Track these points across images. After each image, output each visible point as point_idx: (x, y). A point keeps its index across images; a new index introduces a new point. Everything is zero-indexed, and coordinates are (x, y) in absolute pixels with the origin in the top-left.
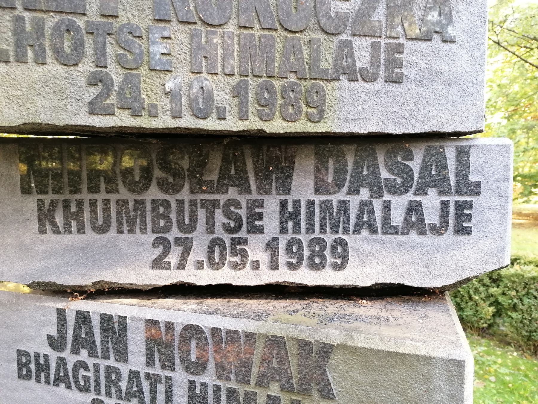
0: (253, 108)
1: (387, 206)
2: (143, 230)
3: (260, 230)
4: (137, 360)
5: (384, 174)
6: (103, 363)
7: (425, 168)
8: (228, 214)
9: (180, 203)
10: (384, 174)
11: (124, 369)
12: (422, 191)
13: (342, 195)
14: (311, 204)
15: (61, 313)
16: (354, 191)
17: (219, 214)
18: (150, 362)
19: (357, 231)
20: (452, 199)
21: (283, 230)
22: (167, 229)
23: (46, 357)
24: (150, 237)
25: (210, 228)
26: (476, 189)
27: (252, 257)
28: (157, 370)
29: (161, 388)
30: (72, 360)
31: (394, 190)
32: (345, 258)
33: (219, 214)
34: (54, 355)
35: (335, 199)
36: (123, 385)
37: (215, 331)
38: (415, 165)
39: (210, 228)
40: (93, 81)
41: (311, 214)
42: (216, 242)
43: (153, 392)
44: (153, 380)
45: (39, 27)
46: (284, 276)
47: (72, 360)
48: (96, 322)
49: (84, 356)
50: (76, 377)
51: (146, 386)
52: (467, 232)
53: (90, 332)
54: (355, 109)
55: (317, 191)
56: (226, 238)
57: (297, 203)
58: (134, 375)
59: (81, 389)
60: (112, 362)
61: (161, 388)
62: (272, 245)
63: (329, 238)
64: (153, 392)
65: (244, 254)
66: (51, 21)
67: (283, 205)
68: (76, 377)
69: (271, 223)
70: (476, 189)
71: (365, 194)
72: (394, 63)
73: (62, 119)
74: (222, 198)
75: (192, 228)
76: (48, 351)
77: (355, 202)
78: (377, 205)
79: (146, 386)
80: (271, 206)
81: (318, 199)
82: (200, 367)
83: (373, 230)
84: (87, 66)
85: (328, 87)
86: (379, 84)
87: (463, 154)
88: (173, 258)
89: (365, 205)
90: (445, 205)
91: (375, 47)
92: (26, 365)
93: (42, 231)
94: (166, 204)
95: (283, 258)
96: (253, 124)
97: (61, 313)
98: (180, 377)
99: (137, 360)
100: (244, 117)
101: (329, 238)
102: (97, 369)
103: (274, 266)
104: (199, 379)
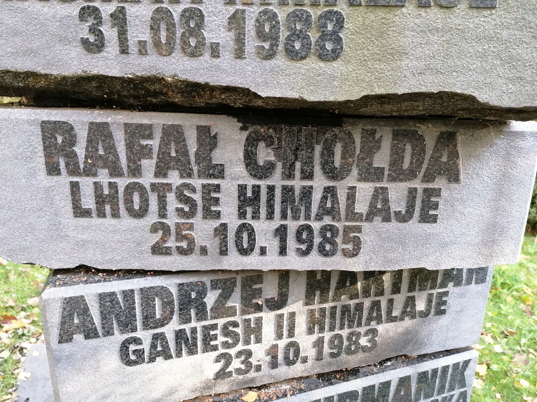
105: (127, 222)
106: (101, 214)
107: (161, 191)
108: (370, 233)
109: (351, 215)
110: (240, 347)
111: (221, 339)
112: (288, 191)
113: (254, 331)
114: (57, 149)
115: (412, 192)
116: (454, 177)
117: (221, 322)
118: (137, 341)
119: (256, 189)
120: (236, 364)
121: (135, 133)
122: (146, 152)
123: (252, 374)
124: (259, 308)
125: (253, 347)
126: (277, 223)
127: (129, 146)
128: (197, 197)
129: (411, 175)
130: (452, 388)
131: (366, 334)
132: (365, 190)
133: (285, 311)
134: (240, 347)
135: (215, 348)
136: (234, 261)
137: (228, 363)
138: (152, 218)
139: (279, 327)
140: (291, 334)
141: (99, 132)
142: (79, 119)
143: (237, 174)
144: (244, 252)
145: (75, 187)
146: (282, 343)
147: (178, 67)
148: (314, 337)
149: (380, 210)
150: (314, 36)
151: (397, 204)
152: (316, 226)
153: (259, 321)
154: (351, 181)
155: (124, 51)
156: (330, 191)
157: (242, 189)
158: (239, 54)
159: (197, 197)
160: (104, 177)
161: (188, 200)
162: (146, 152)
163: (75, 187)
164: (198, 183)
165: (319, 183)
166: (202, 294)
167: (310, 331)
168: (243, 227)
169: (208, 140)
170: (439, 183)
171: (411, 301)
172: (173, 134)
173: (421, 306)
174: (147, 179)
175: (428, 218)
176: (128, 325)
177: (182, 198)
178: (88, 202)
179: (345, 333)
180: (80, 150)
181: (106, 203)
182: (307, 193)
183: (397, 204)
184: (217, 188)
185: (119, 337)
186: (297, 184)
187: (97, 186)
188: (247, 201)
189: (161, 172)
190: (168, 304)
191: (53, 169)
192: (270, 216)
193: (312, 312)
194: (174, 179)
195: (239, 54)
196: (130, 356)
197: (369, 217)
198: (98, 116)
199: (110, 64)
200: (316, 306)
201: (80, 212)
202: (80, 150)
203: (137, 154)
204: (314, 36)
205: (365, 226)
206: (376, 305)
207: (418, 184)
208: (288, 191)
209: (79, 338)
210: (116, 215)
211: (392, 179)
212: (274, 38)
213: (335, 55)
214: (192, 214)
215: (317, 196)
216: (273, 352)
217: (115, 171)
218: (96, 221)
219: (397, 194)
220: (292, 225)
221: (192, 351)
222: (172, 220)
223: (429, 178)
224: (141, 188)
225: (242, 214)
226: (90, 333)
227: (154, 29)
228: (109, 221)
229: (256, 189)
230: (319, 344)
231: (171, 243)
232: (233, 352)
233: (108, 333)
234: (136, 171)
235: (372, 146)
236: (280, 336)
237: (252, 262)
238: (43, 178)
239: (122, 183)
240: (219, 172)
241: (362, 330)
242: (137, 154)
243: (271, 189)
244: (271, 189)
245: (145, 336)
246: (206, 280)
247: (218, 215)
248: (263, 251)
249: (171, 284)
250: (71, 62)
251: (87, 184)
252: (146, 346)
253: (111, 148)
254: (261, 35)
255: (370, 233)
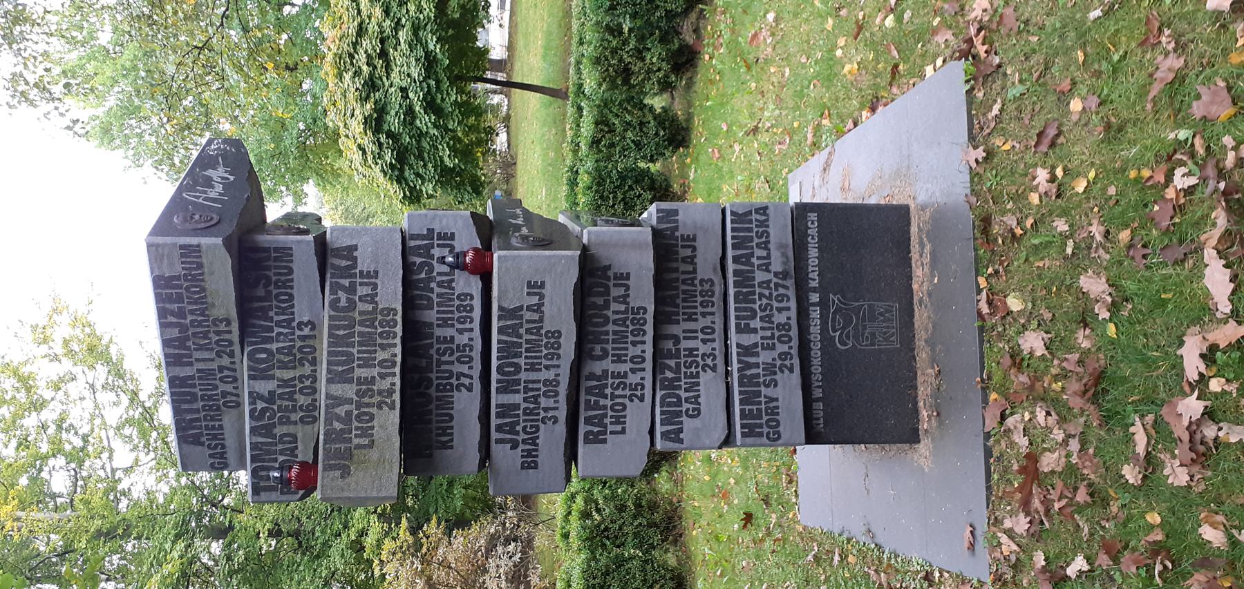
0: (391, 341)
1: (439, 274)
2: (452, 397)
3: (452, 338)
4: (518, 398)
5: (423, 275)
6: (522, 418)
7: (420, 255)
8: (444, 354)
9: (437, 378)
10: (423, 275)
11: (524, 405)
12: (432, 257)
13: (434, 297)
14: (438, 312)
15: (498, 441)
16: (432, 290)
17: (443, 359)
18: (518, 392)
19: (453, 289)
20: (436, 242)
21: (453, 326)
22: (451, 385)
23: (523, 451)
24: (456, 393)
25: (452, 363)
26: (431, 231)
27: (466, 341)
28: (521, 387)
29: (530, 386)
30: (522, 436)
31: (431, 270)
32: (468, 294)
33: (443, 359)
34: (521, 447)
35: (436, 300)
36: (532, 406)
37: (498, 359)
38: (418, 260)
39: (452, 363)
40: (380, 408)
41: (444, 312)
42: (459, 360)
43: (532, 390)
44: (526, 390)
45: (357, 428)
46: (476, 325)
47: (522, 436)
48: (500, 421)
49: (518, 428)
50: (531, 433)
51: (531, 394)
52: (453, 234)
53: (506, 424)
54: (391, 294)
55: (432, 309)
56: (457, 355)
57: (438, 319)
58: (525, 400)
59: (538, 430)
60: (521, 412)
61: (530, 386)
62: (460, 331)
63: (457, 303)
64: (532, 390)
65: (465, 345)
66: (355, 424)
67: (439, 326)
68: (531, 433)
69: (449, 332)
70: (431, 231)
71: (433, 285)
72: (368, 275)
73: (397, 421)
74: (435, 356)
75: (451, 372)
76: (519, 449)
77: (437, 290)
78: (439, 279)
79: (531, 394)
80: (439, 332)
81: (436, 309)
82: (517, 366)
83: (453, 280)
84: (374, 410)
85: (380, 307)
86: (378, 282)
87: (413, 237)
88: (466, 381)
89: (440, 285)
90: (438, 245)
91: (361, 284)
92: (529, 463)
93: (452, 447)
94: (438, 385)
95: (467, 326)
96: (398, 341)
97: (498, 441)
98: (523, 376)
99: (518, 398)
100: (395, 345)
101: (457, 303)
102: (524, 421)
103: (471, 330)
104: (523, 367)
105: (628, 412)
106: (624, 423)
107: (613, 397)
108: (634, 302)
109: (626, 312)
110: (699, 359)
111: (693, 369)
112: (614, 341)
113: (691, 352)
114: (596, 439)
115: (615, 285)
116: (609, 267)
117: (683, 369)
118: (688, 410)
119: (613, 355)
120: (709, 361)
121: (588, 406)
122: (596, 402)
123: (717, 353)
124: (678, 350)
125: (700, 353)
126: (629, 346)
127: (594, 409)
128: (617, 381)
129: (607, 288)
130: (751, 222)
131: (701, 285)
132: (614, 306)
133: (682, 335)
134: (699, 359)
135: (698, 373)
136: (648, 365)
137: (708, 366)
138: (626, 401)
139: (689, 338)
140: (696, 331)
141: (588, 421)
142: (583, 429)
143: (608, 365)
144: (644, 360)
145: (611, 433)
146: (701, 336)
147: (563, 389)
148: (699, 317)
149: (624, 299)
150: (552, 340)
151: (622, 291)
152: (631, 328)
153: (685, 350)
154: (610, 313)
155: (557, 408)
156: (614, 322)
157: (613, 362)
158: (558, 366)
159: (617, 381)
160: (607, 421)
161: (618, 385)
162: (596, 402)
163: (611, 433)
164: (610, 381)
165: (611, 327)
166: (666, 379)
167: (696, 320)
168: (632, 361)
169: (592, 377)
170: (610, 273)
171: (684, 260)
172: (589, 391)
173: (688, 252)
174: (609, 403)
175: (628, 277)
176: (679, 414)
177: (617, 388)
178: (619, 428)
179: (699, 299)
180: (596, 429)
181: (619, 420)
182: (615, 333)
183: (622, 291)
184: (613, 372)
185: (684, 418)
186: (611, 337)
187: (611, 423)
188: (619, 359)
189: (605, 397)
190: (669, 396)
191: (604, 441)
192: (627, 349)
193: (684, 320)
194: (608, 391)
195: (558, 366)
196: (696, 413)
197: (628, 303)
198: (582, 420)
199: (562, 414)
200: (681, 318)
201: (623, 432)
202: (596, 429)
203: (597, 406)
204: (552, 340)
205: (631, 305)
206: (684, 282)
207: (611, 284)
208: (614, 341)
209: (682, 436)
210: (625, 417)
211: (609, 295)
212: (553, 354)
213: (559, 332)
214: (625, 384)
215: (617, 328)
216: (704, 341)
217: (605, 416)
218: (627, 425)
219: (616, 292)
220: (631, 338)
221: (698, 384)
222: (628, 393)
223: (608, 279)
224: (613, 405)
225: (625, 361)
226: (681, 430)
227: (549, 397)
228: (627, 419)
229: (613, 355)
230: (704, 315)
231: (639, 393)
232: (701, 363)
233: (681, 423)
234: (605, 407)
235: (595, 306)
236: (696, 338)
237: (649, 355)
238: (608, 445)
239: (610, 413)
240: (605, 372)
241: (699, 288)
242: (597, 406)
243: (613, 349)
244: (613, 349)
245: (685, 406)
246: (659, 377)
247: (626, 373)
248: (643, 351)
249: (659, 394)
250: (561, 429)
251: (610, 428)
252: (691, 406)
253: (595, 417)
254: (552, 359)
255: (634, 302)
